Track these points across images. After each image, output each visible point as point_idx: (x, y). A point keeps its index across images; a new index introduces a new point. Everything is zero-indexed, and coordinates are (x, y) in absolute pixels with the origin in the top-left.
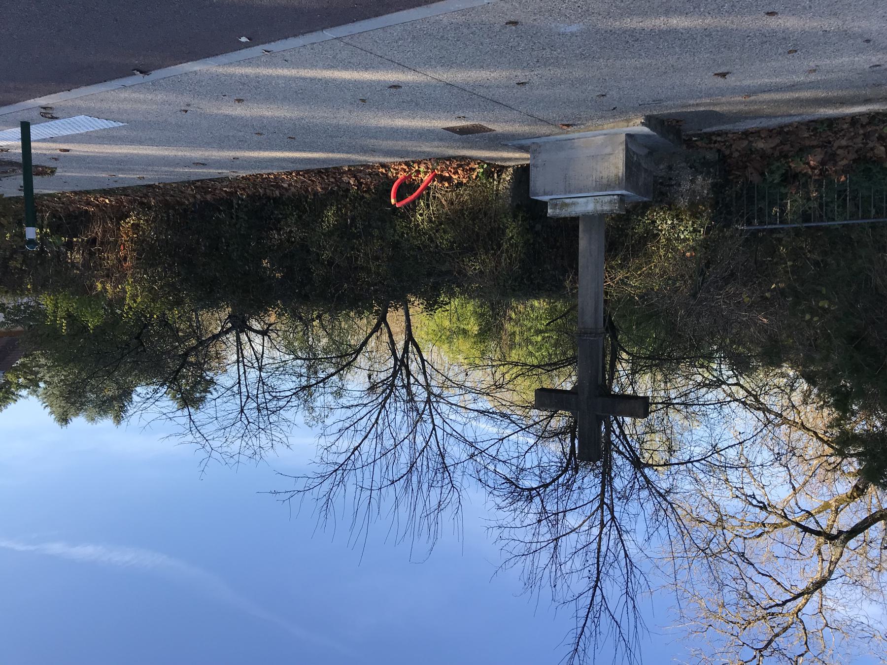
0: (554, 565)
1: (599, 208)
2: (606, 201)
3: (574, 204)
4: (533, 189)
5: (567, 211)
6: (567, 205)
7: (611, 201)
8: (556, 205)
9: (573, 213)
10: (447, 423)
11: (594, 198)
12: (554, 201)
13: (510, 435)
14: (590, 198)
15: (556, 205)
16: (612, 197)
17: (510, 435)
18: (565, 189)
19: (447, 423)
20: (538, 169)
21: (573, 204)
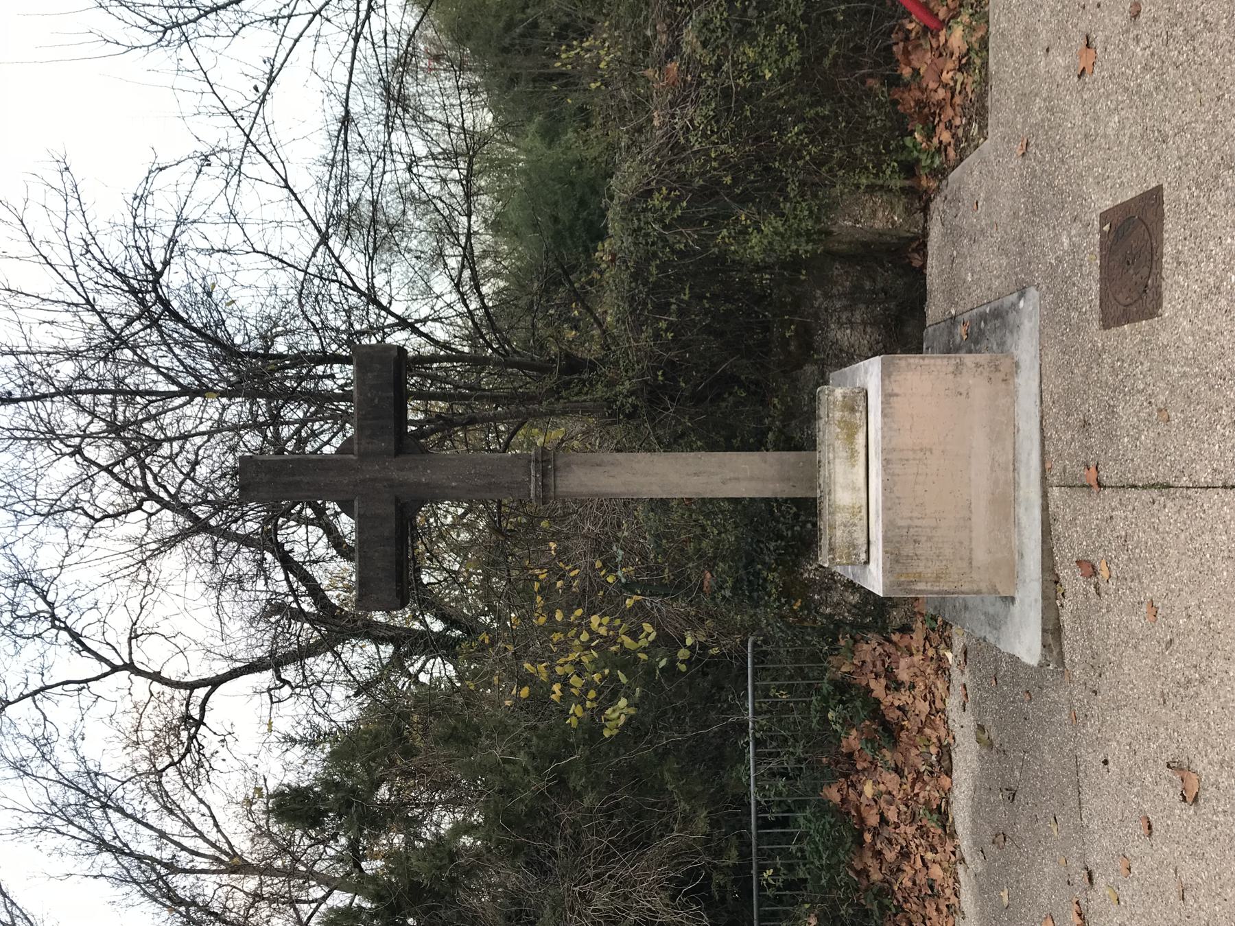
0: (211, 851)
1: (840, 518)
2: (855, 535)
3: (852, 456)
4: (903, 363)
5: (837, 438)
6: (851, 437)
7: (855, 547)
8: (853, 410)
9: (831, 455)
10: (310, 22)
11: (864, 503)
12: (862, 404)
13: (299, 202)
14: (865, 496)
15: (853, 410)
16: (864, 548)
17: (299, 202)
18: (894, 450)
19: (310, 22)
20: (951, 376)
21: (853, 454)
